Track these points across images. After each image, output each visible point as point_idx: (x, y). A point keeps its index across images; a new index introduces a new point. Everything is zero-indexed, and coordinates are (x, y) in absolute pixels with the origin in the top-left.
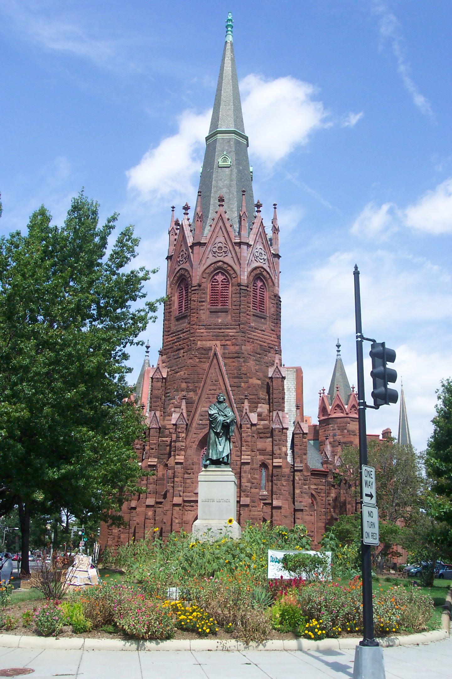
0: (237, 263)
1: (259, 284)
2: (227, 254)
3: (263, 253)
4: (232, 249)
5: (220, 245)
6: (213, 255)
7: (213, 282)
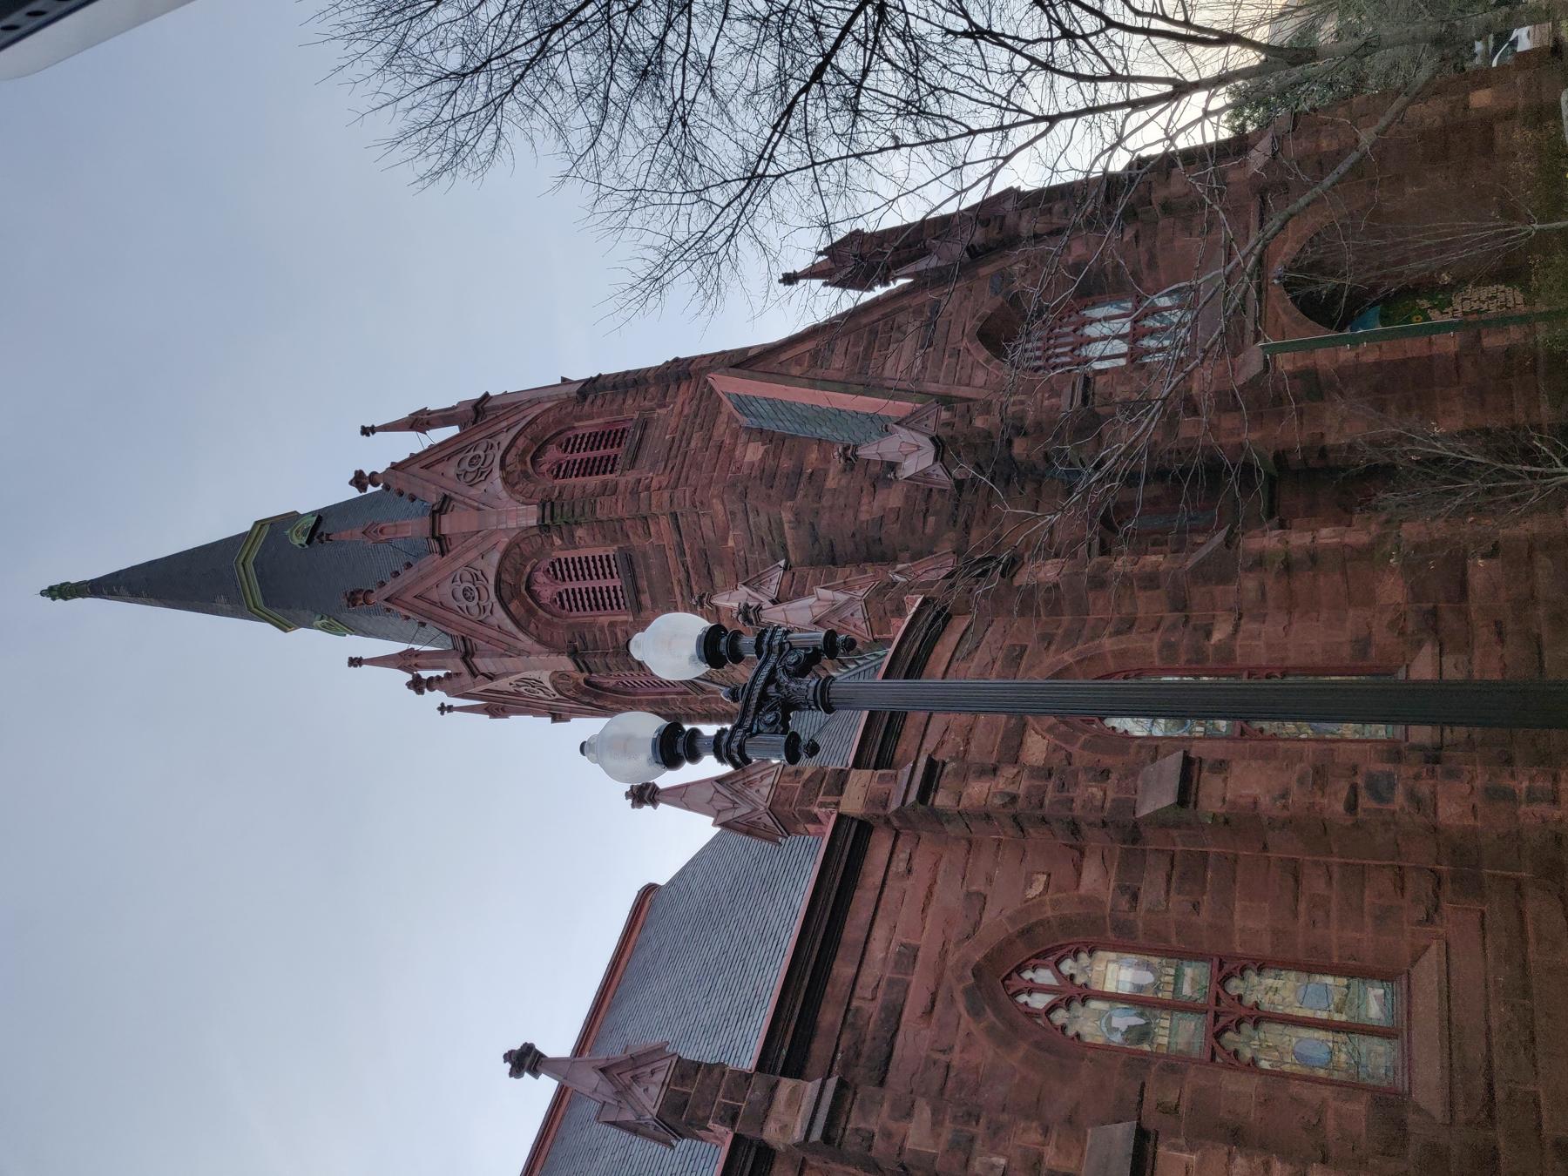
0: (493, 540)
1: (553, 454)
2: (479, 573)
3: (472, 454)
4: (461, 562)
5: (459, 594)
6: (488, 612)
7: (563, 606)
